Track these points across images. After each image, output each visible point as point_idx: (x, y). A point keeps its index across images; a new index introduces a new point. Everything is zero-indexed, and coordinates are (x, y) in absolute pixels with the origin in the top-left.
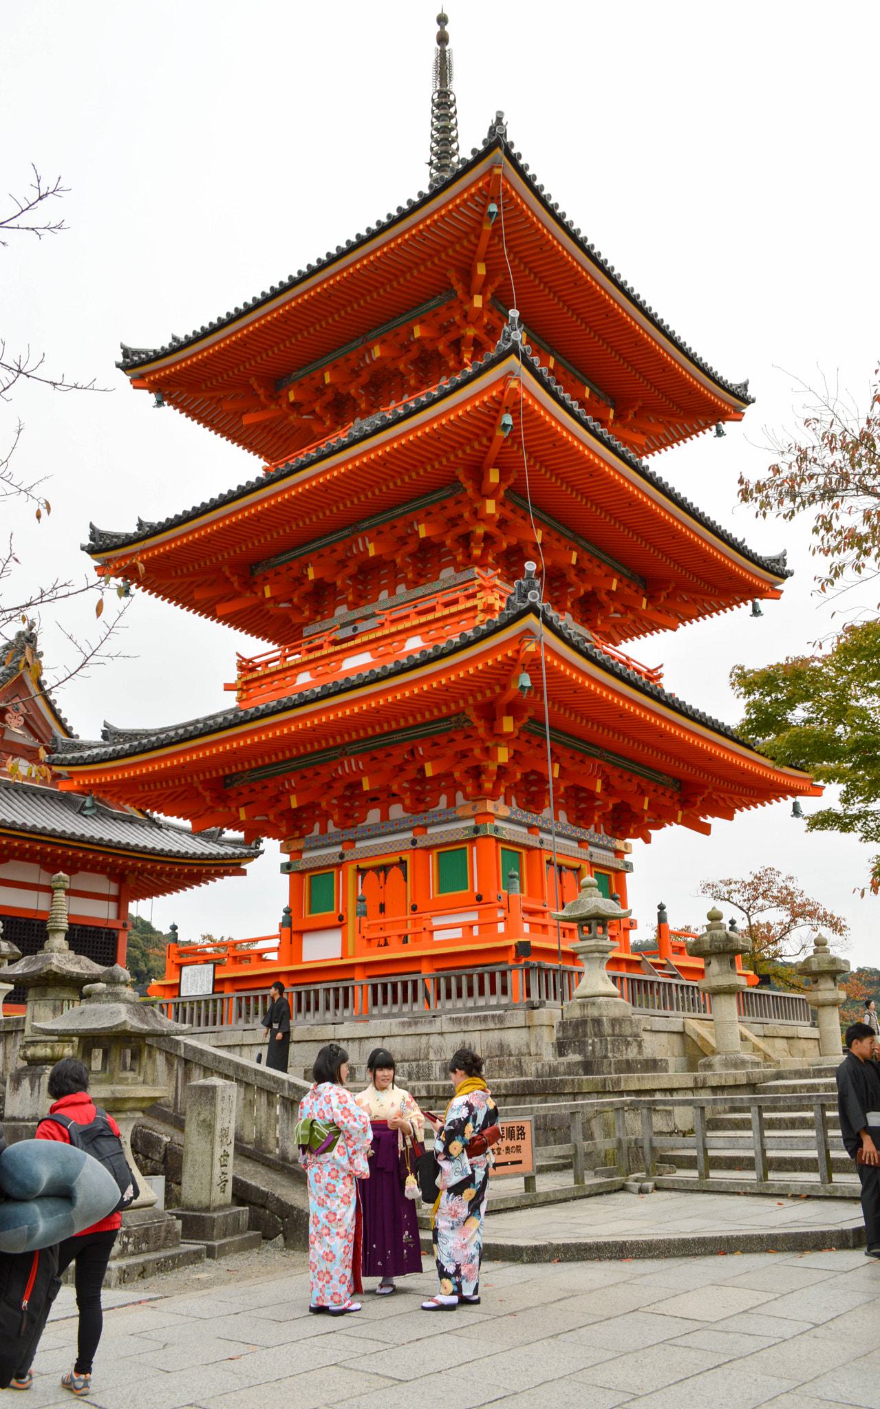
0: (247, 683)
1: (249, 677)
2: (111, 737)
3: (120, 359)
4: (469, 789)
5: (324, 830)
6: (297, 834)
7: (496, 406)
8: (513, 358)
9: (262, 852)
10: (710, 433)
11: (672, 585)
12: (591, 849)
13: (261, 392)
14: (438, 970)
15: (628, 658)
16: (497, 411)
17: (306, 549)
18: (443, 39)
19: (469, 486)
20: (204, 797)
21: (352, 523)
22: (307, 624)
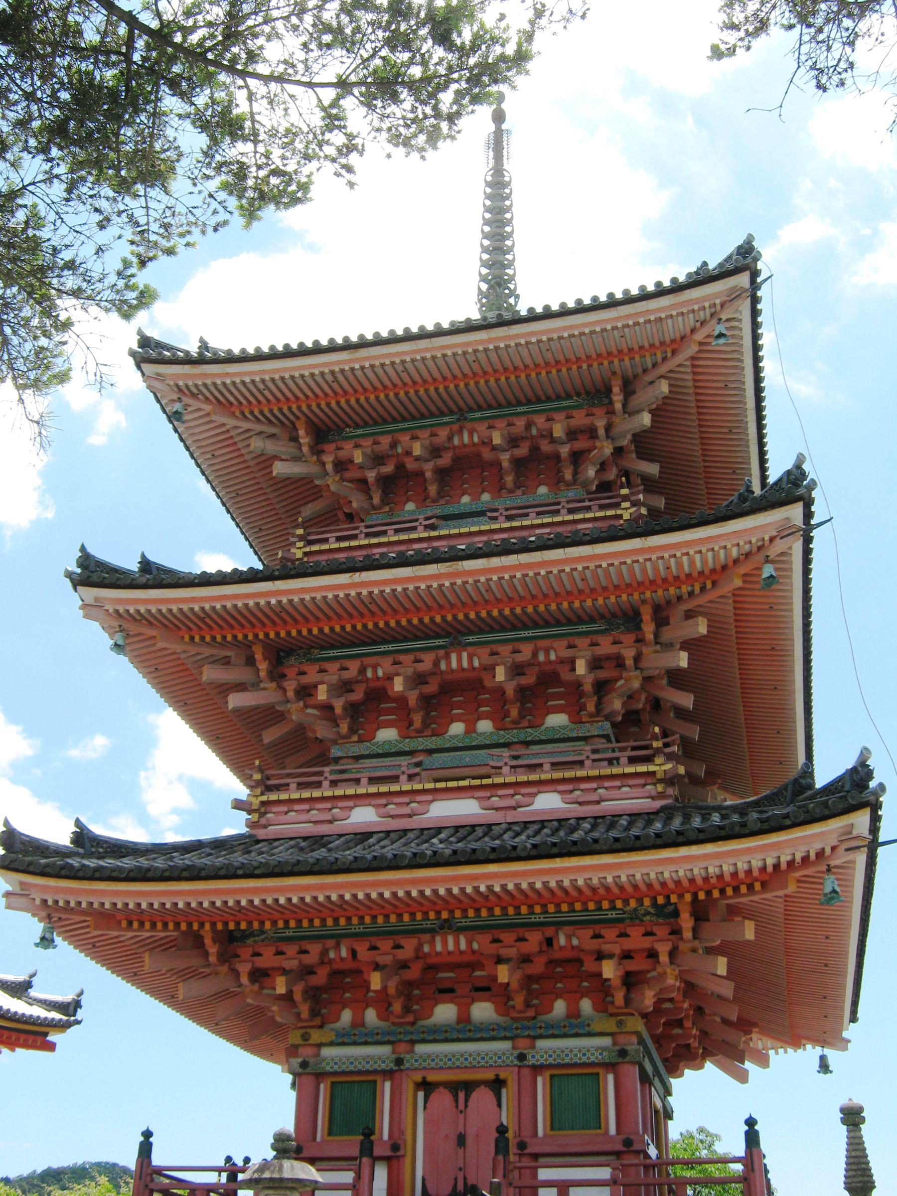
0: (263, 803)
1: (273, 797)
2: (88, 845)
3: (135, 347)
6: (317, 1021)
9: (78, 1022)
20: (206, 954)
21: (455, 634)
22: (335, 742)
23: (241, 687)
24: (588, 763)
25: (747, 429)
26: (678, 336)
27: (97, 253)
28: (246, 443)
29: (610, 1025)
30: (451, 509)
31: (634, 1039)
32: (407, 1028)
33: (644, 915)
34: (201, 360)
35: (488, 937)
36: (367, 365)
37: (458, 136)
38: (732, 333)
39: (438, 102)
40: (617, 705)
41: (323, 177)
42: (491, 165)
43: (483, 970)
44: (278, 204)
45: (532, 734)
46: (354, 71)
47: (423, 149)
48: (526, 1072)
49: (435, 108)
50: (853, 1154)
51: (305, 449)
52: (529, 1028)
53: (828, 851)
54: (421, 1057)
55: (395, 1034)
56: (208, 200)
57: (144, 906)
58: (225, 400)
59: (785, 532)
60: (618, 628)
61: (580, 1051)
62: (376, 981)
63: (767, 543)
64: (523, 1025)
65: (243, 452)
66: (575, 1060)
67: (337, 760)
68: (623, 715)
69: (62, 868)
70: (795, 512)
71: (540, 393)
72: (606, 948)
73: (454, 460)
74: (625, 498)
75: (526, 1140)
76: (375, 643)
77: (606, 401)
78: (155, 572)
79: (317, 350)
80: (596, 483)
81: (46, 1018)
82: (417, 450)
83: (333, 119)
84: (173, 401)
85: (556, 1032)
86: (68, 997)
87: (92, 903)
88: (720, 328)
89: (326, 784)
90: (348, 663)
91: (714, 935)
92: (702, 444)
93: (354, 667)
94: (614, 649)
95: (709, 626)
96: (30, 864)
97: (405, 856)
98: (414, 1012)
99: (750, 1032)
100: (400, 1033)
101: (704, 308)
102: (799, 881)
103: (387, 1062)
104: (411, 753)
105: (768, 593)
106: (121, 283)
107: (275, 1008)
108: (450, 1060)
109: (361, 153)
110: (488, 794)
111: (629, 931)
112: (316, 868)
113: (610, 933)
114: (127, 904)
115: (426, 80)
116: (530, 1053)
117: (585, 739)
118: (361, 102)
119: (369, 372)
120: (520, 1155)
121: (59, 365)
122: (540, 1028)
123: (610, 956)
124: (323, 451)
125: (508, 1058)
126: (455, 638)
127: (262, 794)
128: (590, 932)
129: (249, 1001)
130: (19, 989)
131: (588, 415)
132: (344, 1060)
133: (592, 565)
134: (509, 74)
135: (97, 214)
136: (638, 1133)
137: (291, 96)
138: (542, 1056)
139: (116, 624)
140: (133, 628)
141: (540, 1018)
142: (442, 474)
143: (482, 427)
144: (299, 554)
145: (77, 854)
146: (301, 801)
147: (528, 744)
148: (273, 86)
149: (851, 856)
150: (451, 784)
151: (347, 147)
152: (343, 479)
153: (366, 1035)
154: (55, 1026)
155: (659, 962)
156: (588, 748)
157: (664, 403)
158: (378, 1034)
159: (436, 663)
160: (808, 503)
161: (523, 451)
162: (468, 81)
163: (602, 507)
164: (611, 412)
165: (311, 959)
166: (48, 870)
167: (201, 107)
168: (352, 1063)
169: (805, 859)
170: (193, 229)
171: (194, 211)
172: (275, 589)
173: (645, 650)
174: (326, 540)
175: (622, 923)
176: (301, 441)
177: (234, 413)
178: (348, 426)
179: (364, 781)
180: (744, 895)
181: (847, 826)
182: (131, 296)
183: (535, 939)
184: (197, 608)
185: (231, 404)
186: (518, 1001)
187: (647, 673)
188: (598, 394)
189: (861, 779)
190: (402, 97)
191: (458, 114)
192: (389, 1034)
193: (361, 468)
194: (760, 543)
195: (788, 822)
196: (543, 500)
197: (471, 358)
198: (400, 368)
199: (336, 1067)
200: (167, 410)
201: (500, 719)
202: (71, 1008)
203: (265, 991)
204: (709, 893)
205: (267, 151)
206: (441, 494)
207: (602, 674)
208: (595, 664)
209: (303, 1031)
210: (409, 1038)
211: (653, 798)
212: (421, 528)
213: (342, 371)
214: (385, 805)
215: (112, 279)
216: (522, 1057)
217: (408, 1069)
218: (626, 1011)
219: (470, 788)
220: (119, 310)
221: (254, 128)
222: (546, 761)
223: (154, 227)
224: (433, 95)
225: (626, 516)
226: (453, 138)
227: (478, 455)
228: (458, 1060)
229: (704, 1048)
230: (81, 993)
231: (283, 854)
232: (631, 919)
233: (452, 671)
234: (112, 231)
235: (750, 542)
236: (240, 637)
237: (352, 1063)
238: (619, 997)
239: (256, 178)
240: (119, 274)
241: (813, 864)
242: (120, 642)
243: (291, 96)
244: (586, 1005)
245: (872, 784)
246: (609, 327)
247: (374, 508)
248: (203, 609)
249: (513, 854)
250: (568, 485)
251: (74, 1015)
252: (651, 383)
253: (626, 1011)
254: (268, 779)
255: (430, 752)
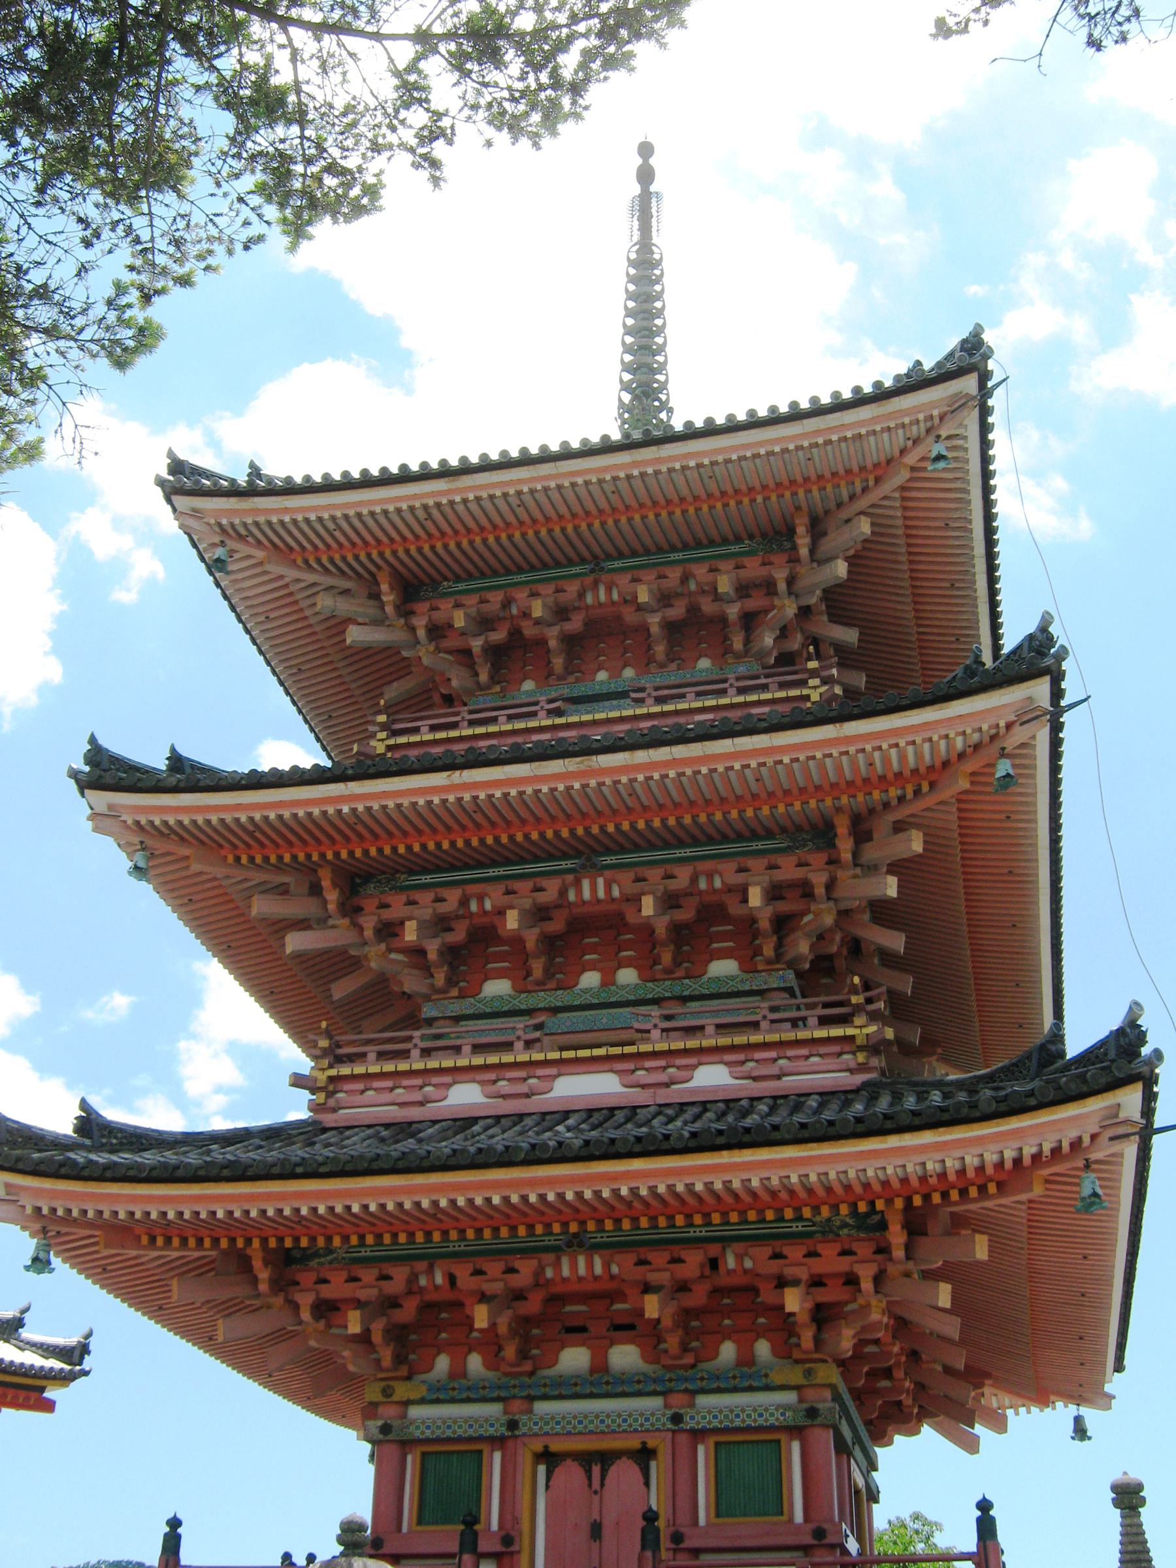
0: (331, 1079)
1: (345, 1070)
2: (96, 1133)
3: (164, 474)
6: (404, 1371)
9: (86, 1373)
18: (646, 175)
20: (255, 1281)
21: (588, 853)
22: (427, 998)
23: (302, 924)
24: (764, 1025)
25: (974, 583)
26: (883, 459)
27: (78, 274)
28: (311, 601)
29: (795, 1376)
30: (582, 689)
31: (828, 1394)
32: (524, 1381)
33: (840, 1228)
34: (251, 491)
35: (632, 1258)
36: (471, 497)
37: (585, 114)
38: (955, 454)
39: (555, 69)
40: (803, 947)
41: (397, 174)
42: (636, 238)
43: (625, 1302)
44: (335, 214)
45: (690, 986)
46: (439, 17)
47: (537, 135)
48: (683, 1439)
49: (555, 75)
50: (1130, 1548)
51: (389, 609)
52: (686, 1380)
53: (1086, 1140)
54: (541, 1418)
55: (507, 1388)
56: (237, 206)
57: (171, 1215)
58: (283, 544)
59: (1027, 716)
60: (804, 846)
61: (755, 1410)
62: (481, 1317)
63: (1003, 731)
64: (679, 1377)
65: (308, 613)
66: (749, 1422)
67: (430, 1022)
68: (812, 962)
69: (62, 1165)
70: (1040, 689)
71: (701, 535)
72: (789, 1272)
73: (586, 624)
74: (814, 673)
75: (682, 1530)
76: (480, 865)
77: (787, 545)
78: (188, 770)
79: (405, 477)
80: (775, 654)
81: (42, 1368)
82: (537, 609)
83: (412, 91)
84: (214, 545)
85: (723, 1385)
86: (73, 1340)
87: (101, 1212)
88: (939, 448)
89: (415, 1053)
90: (445, 893)
91: (934, 1254)
92: (916, 603)
93: (453, 897)
94: (799, 873)
95: (925, 842)
96: (19, 1159)
97: (521, 1148)
98: (532, 1357)
99: (981, 1385)
100: (514, 1387)
101: (918, 422)
102: (1047, 1181)
103: (497, 1425)
104: (529, 1012)
105: (1002, 798)
106: (112, 316)
107: (346, 1353)
108: (580, 1422)
109: (450, 142)
110: (632, 1066)
111: (820, 1248)
112: (400, 1165)
113: (795, 1252)
114: (148, 1214)
115: (540, 33)
116: (687, 1413)
117: (761, 993)
118: (450, 63)
119: (473, 507)
120: (675, 1550)
121: (27, 434)
122: (702, 1379)
123: (795, 1283)
124: (413, 613)
125: (658, 1420)
126: (589, 859)
127: (331, 1066)
128: (768, 1251)
129: (313, 1343)
130: (7, 1329)
131: (764, 564)
132: (439, 1423)
133: (770, 761)
134: (657, 26)
135: (81, 227)
136: (832, 1520)
137: (352, 55)
138: (704, 1418)
139: (136, 840)
140: (160, 846)
141: (701, 1366)
142: (571, 642)
143: (624, 580)
144: (380, 748)
145: (82, 1147)
146: (382, 1075)
147: (684, 999)
148: (329, 40)
149: (1116, 1147)
150: (583, 1053)
151: (431, 132)
152: (438, 650)
153: (469, 1389)
154: (54, 1378)
155: (860, 1291)
156: (765, 1005)
157: (864, 548)
158: (484, 1388)
159: (563, 893)
160: (1057, 677)
161: (677, 611)
162: (599, 35)
163: (783, 686)
164: (794, 560)
165: (397, 1285)
166: (43, 1167)
167: (228, 74)
168: (449, 1427)
169: (1056, 1151)
170: (216, 246)
171: (216, 219)
172: (347, 793)
173: (840, 874)
174: (416, 730)
175: (811, 1238)
176: (384, 598)
177: (294, 561)
178: (446, 579)
179: (467, 1049)
180: (975, 1200)
181: (1111, 1107)
182: (125, 334)
183: (694, 1260)
184: (243, 819)
185: (291, 549)
186: (672, 1343)
187: (843, 906)
188: (777, 536)
189: (1130, 1044)
190: (507, 58)
191: (587, 80)
192: (499, 1388)
193: (463, 634)
194: (993, 731)
195: (1032, 1102)
196: (704, 677)
197: (609, 488)
198: (514, 501)
199: (428, 1433)
200: (206, 557)
201: (647, 967)
202: (75, 1354)
203: (334, 1331)
204: (927, 1198)
205: (319, 137)
206: (569, 670)
207: (784, 907)
208: (774, 893)
209: (384, 1384)
210: (524, 1394)
211: (851, 1071)
212: (542, 714)
213: (438, 505)
214: (495, 1082)
215: (99, 310)
216: (677, 1419)
217: (524, 1435)
219: (608, 1058)
220: (110, 355)
221: (300, 103)
222: (709, 1022)
223: (162, 244)
224: (550, 56)
225: (815, 697)
226: (577, 116)
227: (619, 618)
228: (592, 1422)
229: (920, 1407)
230: (89, 1335)
231: (357, 1146)
232: (823, 1233)
233: (584, 903)
234: (99, 247)
235: (980, 730)
236: (301, 857)
237: (449, 1427)
238: (807, 1337)
239: (304, 176)
240: (110, 303)
241: (1066, 1158)
242: (142, 864)
243: (352, 55)
244: (763, 1349)
245: (1145, 1051)
246: (791, 447)
247: (480, 687)
248: (251, 819)
249: (665, 1146)
250: (738, 657)
251: (80, 1364)
252: (848, 521)
253: (816, 1356)
254: (339, 1046)
255: (555, 1010)
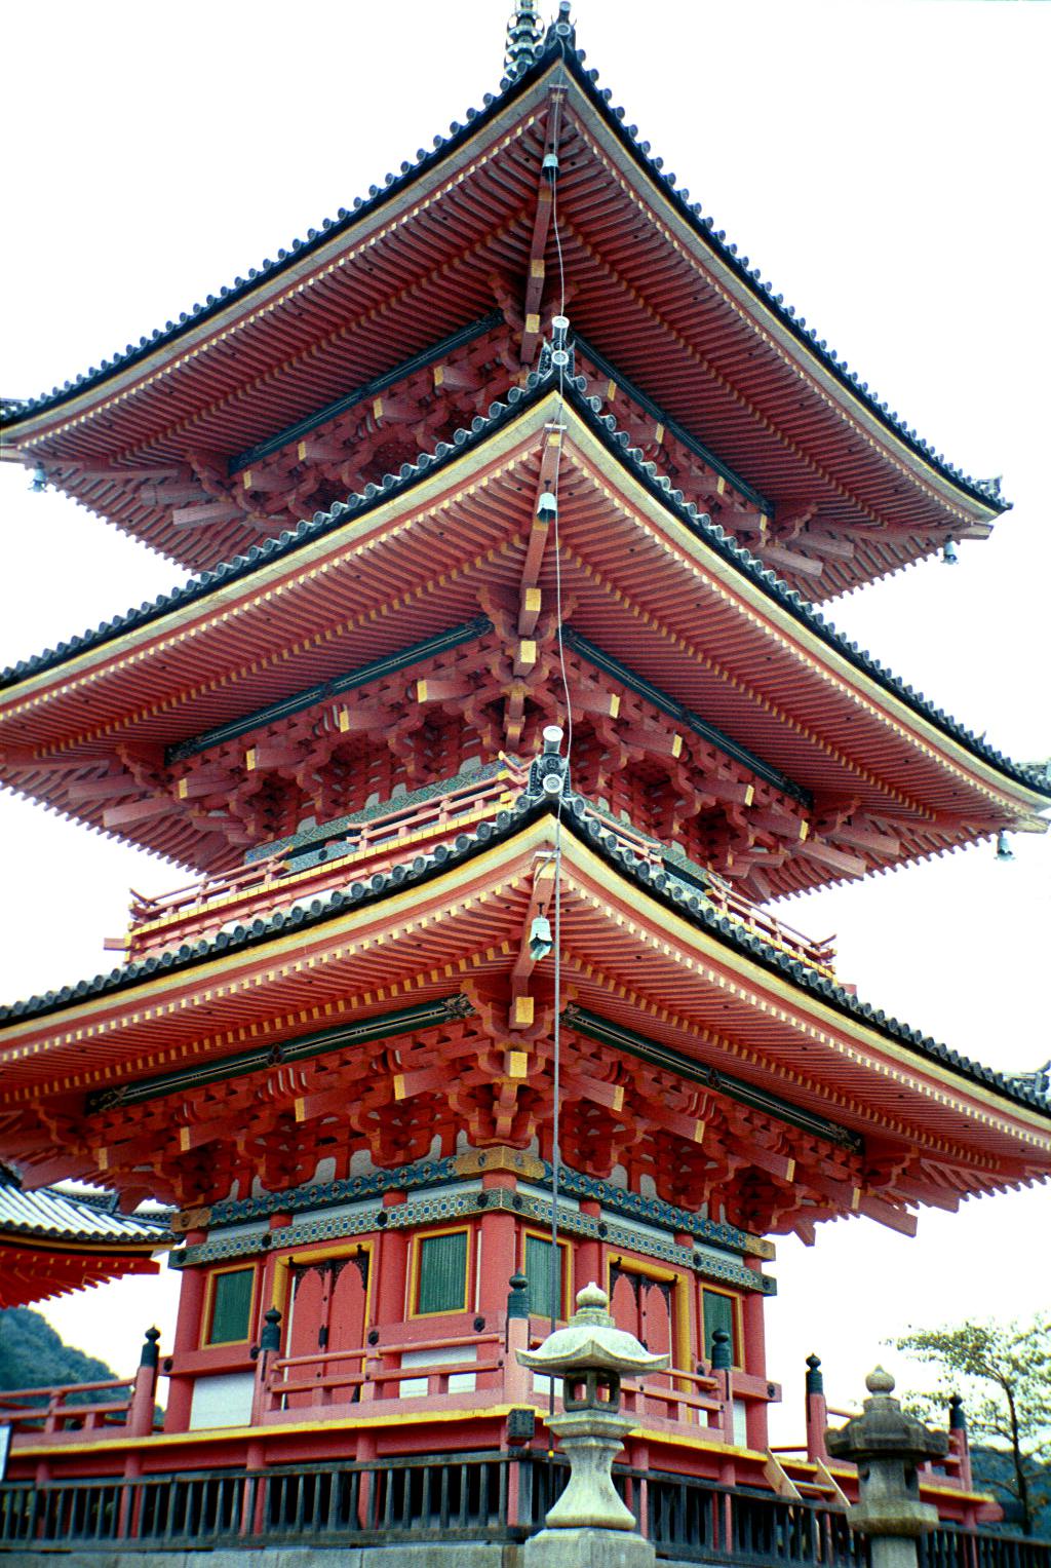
0: (142, 938)
4: (474, 1127)
5: (246, 1192)
6: (201, 1200)
7: (530, 480)
8: (556, 397)
10: (935, 560)
11: (855, 803)
12: (698, 1248)
13: (204, 475)
14: (382, 1456)
15: (774, 921)
16: (534, 489)
17: (249, 723)
19: (498, 618)
20: (48, 1130)
22: (249, 847)
51: (206, 486)
127: (136, 926)
217: (275, 1249)
218: (493, 1141)
253: (493, 1141)
